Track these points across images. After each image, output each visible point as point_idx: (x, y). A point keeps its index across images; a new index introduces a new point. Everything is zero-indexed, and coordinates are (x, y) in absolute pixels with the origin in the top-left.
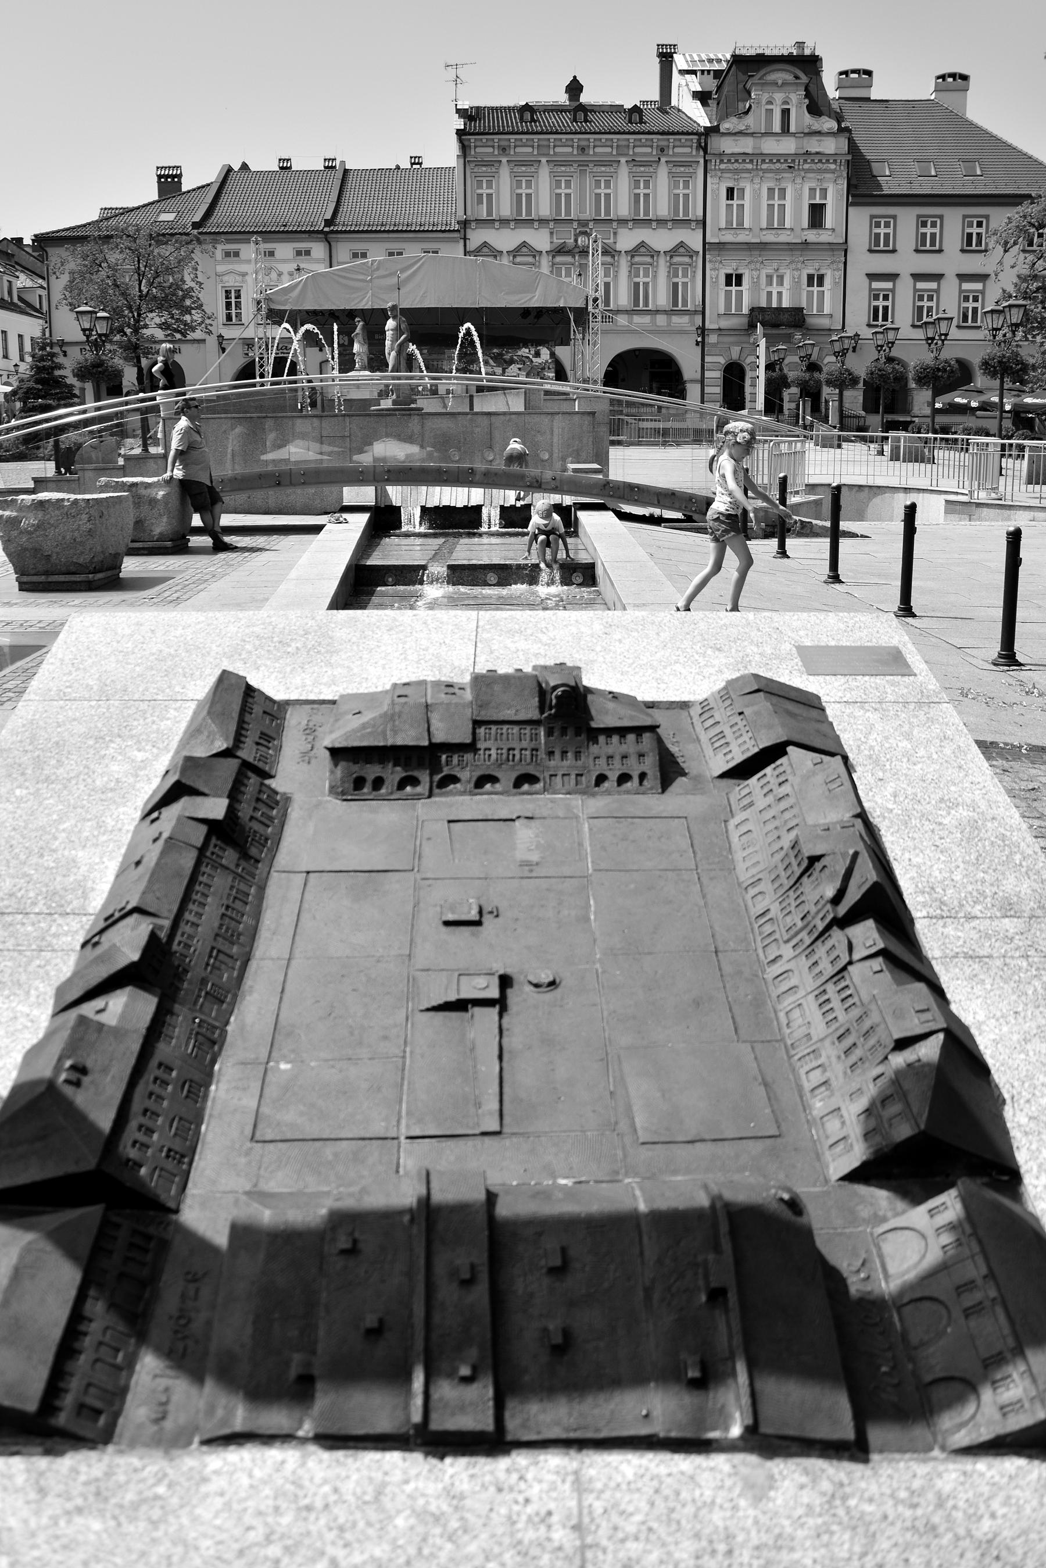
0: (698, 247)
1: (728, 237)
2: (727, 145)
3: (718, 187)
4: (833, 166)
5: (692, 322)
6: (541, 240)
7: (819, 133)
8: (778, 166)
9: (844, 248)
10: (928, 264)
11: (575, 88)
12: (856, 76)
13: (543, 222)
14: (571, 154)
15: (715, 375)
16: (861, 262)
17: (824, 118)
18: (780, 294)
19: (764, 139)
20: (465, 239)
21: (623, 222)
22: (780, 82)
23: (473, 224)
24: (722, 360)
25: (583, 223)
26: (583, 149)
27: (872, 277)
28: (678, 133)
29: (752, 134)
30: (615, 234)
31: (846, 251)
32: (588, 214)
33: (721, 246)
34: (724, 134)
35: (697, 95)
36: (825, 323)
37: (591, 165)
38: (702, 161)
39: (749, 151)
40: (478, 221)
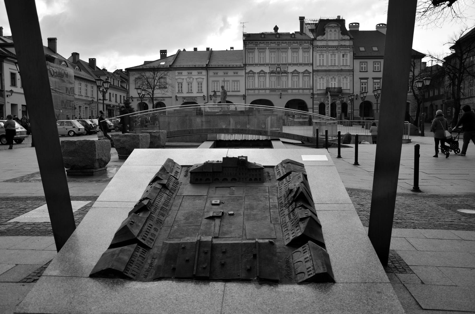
1: (320, 68)
2: (319, 43)
4: (349, 49)
5: (310, 92)
6: (267, 69)
7: (344, 40)
8: (333, 49)
9: (353, 71)
11: (276, 28)
12: (355, 24)
13: (267, 64)
14: (275, 46)
15: (317, 106)
16: (358, 75)
17: (346, 36)
18: (335, 84)
19: (329, 42)
20: (245, 69)
21: (290, 64)
22: (333, 26)
23: (248, 65)
24: (319, 102)
25: (279, 65)
26: (278, 45)
27: (361, 79)
28: (305, 40)
30: (288, 67)
31: (353, 72)
33: (318, 71)
34: (318, 40)
35: (310, 30)
36: (348, 92)
37: (281, 49)
38: (312, 48)
39: (325, 45)
40: (249, 64)
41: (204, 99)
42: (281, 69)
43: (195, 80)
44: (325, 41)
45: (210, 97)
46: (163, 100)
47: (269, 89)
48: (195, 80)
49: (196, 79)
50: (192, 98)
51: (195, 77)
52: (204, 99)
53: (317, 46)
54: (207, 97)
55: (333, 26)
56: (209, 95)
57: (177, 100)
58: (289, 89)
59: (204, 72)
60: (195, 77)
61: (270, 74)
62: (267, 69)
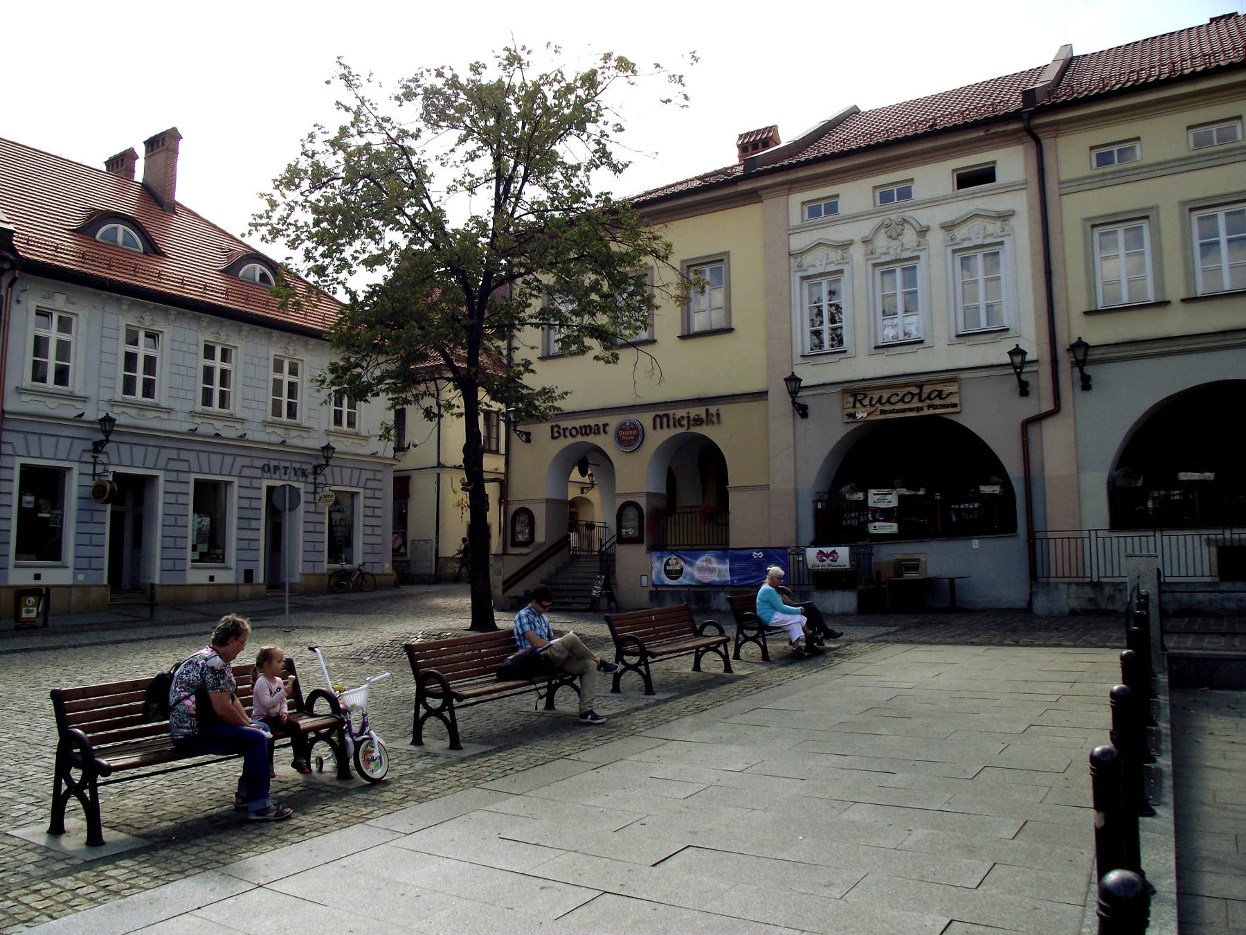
41: (1024, 390)
43: (936, 239)
45: (1080, 364)
46: (709, 420)
48: (936, 239)
49: (948, 227)
50: (917, 383)
51: (934, 217)
52: (1024, 390)
54: (1045, 371)
56: (1061, 350)
57: (802, 411)
60: (934, 217)
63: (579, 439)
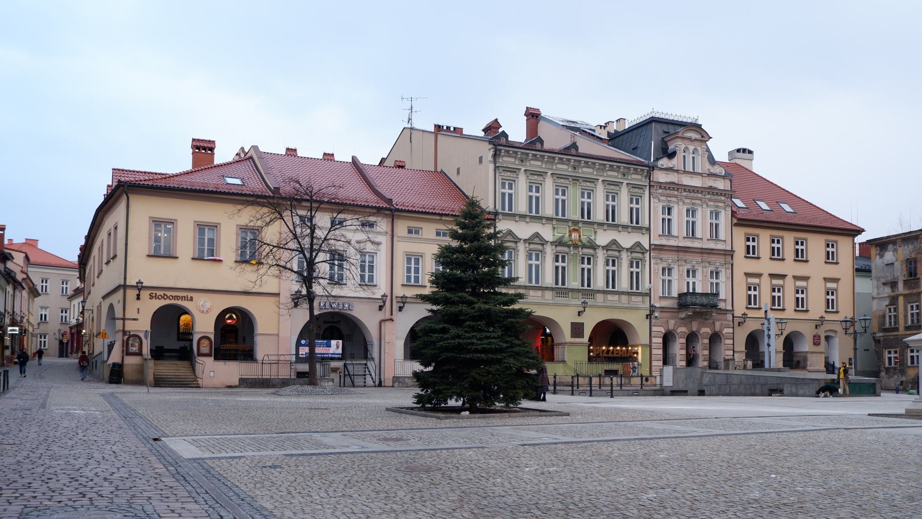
0: (647, 247)
1: (664, 242)
2: (660, 177)
3: (658, 206)
4: (723, 198)
6: (547, 233)
9: (730, 253)
10: (778, 268)
13: (549, 219)
16: (742, 264)
18: (694, 283)
21: (601, 225)
23: (500, 217)
25: (575, 222)
27: (747, 275)
29: (677, 171)
30: (595, 232)
32: (578, 217)
33: (660, 248)
34: (661, 169)
37: (581, 180)
40: (504, 215)
42: (580, 236)
44: (676, 174)
47: (552, 289)
53: (661, 185)
55: (693, 138)
56: (394, 297)
58: (598, 291)
59: (383, 225)
61: (556, 246)
62: (547, 233)
63: (173, 302)
